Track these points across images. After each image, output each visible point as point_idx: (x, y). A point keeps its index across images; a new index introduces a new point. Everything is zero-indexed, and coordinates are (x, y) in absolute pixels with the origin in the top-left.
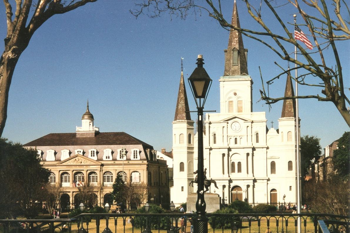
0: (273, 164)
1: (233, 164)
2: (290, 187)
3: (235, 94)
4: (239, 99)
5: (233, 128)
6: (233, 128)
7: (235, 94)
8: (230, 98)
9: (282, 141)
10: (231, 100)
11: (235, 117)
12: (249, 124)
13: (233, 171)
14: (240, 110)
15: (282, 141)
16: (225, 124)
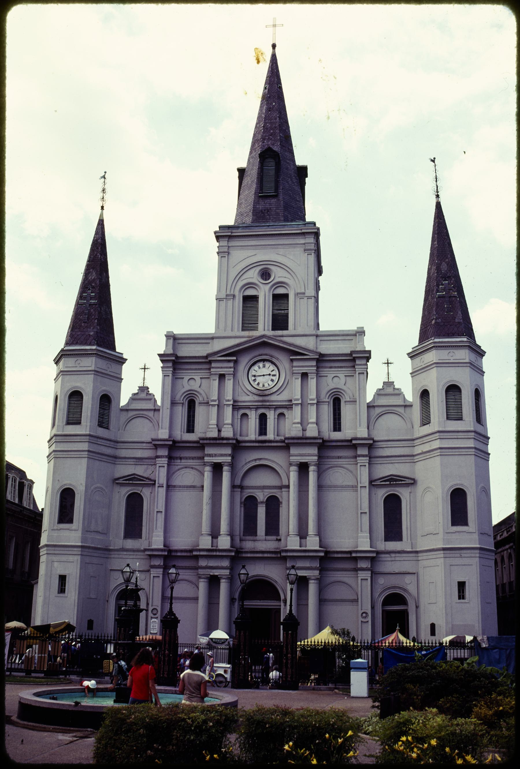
0: (393, 505)
1: (250, 504)
2: (462, 586)
3: (265, 274)
4: (281, 291)
5: (255, 380)
6: (255, 380)
7: (265, 274)
8: (250, 285)
9: (426, 420)
10: (250, 292)
11: (263, 344)
12: (310, 367)
13: (250, 528)
14: (280, 322)
15: (426, 420)
16: (227, 369)
